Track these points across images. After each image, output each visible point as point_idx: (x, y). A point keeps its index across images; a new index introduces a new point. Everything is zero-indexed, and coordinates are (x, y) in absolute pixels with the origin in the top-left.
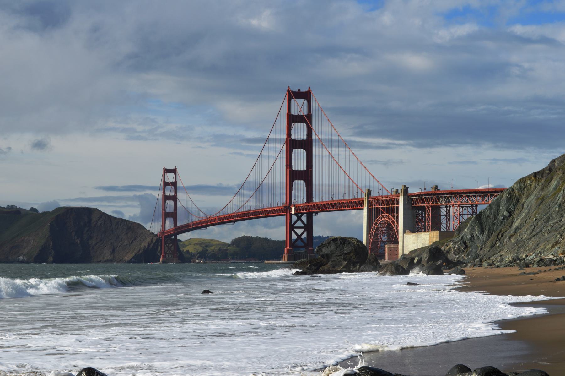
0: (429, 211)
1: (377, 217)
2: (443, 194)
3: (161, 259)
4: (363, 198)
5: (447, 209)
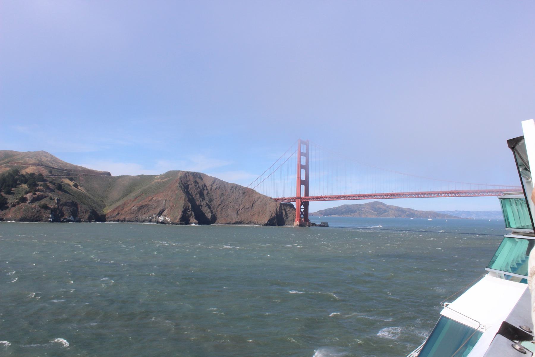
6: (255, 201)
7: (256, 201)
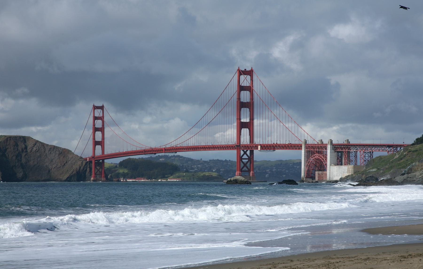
0: (346, 154)
1: (311, 156)
2: (352, 145)
3: (92, 179)
4: (302, 144)
5: (355, 153)
6: (68, 161)
7: (69, 161)
